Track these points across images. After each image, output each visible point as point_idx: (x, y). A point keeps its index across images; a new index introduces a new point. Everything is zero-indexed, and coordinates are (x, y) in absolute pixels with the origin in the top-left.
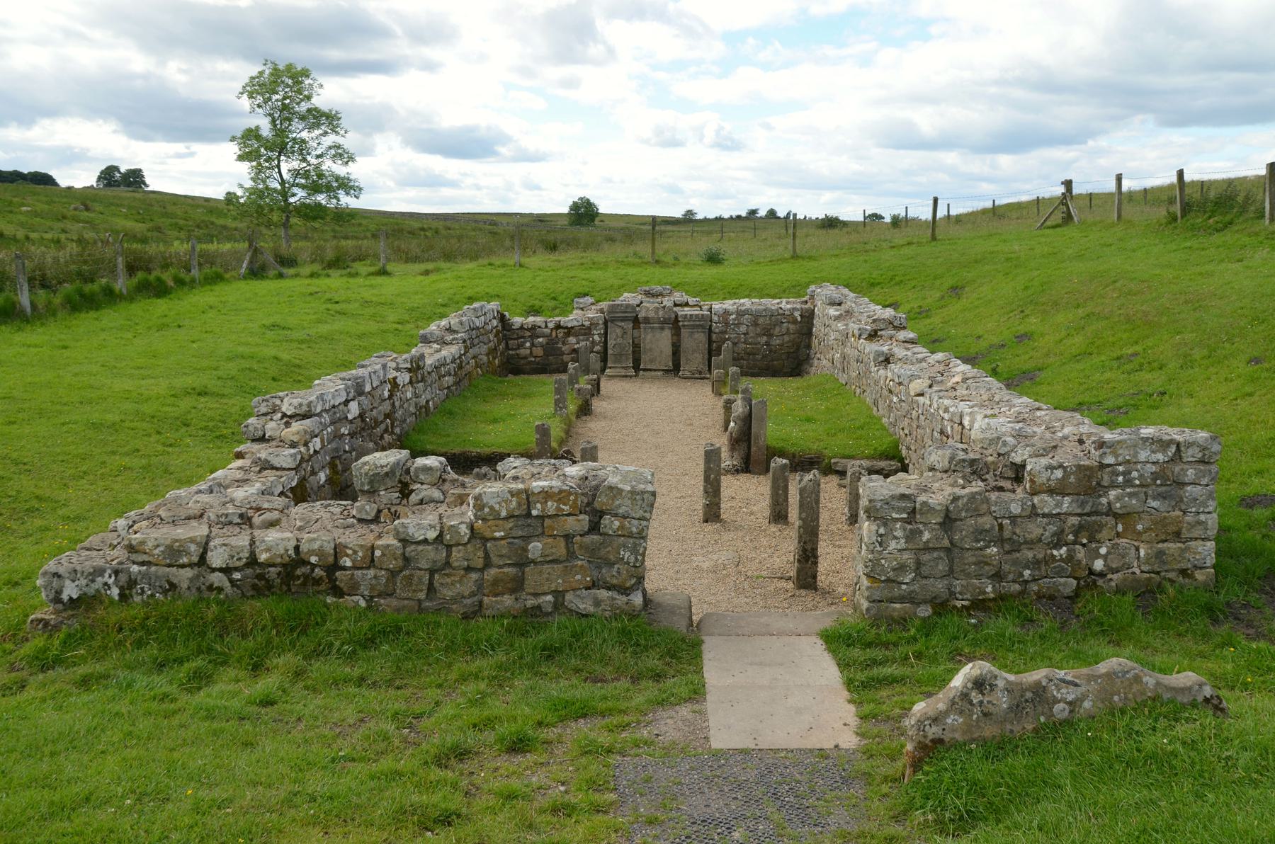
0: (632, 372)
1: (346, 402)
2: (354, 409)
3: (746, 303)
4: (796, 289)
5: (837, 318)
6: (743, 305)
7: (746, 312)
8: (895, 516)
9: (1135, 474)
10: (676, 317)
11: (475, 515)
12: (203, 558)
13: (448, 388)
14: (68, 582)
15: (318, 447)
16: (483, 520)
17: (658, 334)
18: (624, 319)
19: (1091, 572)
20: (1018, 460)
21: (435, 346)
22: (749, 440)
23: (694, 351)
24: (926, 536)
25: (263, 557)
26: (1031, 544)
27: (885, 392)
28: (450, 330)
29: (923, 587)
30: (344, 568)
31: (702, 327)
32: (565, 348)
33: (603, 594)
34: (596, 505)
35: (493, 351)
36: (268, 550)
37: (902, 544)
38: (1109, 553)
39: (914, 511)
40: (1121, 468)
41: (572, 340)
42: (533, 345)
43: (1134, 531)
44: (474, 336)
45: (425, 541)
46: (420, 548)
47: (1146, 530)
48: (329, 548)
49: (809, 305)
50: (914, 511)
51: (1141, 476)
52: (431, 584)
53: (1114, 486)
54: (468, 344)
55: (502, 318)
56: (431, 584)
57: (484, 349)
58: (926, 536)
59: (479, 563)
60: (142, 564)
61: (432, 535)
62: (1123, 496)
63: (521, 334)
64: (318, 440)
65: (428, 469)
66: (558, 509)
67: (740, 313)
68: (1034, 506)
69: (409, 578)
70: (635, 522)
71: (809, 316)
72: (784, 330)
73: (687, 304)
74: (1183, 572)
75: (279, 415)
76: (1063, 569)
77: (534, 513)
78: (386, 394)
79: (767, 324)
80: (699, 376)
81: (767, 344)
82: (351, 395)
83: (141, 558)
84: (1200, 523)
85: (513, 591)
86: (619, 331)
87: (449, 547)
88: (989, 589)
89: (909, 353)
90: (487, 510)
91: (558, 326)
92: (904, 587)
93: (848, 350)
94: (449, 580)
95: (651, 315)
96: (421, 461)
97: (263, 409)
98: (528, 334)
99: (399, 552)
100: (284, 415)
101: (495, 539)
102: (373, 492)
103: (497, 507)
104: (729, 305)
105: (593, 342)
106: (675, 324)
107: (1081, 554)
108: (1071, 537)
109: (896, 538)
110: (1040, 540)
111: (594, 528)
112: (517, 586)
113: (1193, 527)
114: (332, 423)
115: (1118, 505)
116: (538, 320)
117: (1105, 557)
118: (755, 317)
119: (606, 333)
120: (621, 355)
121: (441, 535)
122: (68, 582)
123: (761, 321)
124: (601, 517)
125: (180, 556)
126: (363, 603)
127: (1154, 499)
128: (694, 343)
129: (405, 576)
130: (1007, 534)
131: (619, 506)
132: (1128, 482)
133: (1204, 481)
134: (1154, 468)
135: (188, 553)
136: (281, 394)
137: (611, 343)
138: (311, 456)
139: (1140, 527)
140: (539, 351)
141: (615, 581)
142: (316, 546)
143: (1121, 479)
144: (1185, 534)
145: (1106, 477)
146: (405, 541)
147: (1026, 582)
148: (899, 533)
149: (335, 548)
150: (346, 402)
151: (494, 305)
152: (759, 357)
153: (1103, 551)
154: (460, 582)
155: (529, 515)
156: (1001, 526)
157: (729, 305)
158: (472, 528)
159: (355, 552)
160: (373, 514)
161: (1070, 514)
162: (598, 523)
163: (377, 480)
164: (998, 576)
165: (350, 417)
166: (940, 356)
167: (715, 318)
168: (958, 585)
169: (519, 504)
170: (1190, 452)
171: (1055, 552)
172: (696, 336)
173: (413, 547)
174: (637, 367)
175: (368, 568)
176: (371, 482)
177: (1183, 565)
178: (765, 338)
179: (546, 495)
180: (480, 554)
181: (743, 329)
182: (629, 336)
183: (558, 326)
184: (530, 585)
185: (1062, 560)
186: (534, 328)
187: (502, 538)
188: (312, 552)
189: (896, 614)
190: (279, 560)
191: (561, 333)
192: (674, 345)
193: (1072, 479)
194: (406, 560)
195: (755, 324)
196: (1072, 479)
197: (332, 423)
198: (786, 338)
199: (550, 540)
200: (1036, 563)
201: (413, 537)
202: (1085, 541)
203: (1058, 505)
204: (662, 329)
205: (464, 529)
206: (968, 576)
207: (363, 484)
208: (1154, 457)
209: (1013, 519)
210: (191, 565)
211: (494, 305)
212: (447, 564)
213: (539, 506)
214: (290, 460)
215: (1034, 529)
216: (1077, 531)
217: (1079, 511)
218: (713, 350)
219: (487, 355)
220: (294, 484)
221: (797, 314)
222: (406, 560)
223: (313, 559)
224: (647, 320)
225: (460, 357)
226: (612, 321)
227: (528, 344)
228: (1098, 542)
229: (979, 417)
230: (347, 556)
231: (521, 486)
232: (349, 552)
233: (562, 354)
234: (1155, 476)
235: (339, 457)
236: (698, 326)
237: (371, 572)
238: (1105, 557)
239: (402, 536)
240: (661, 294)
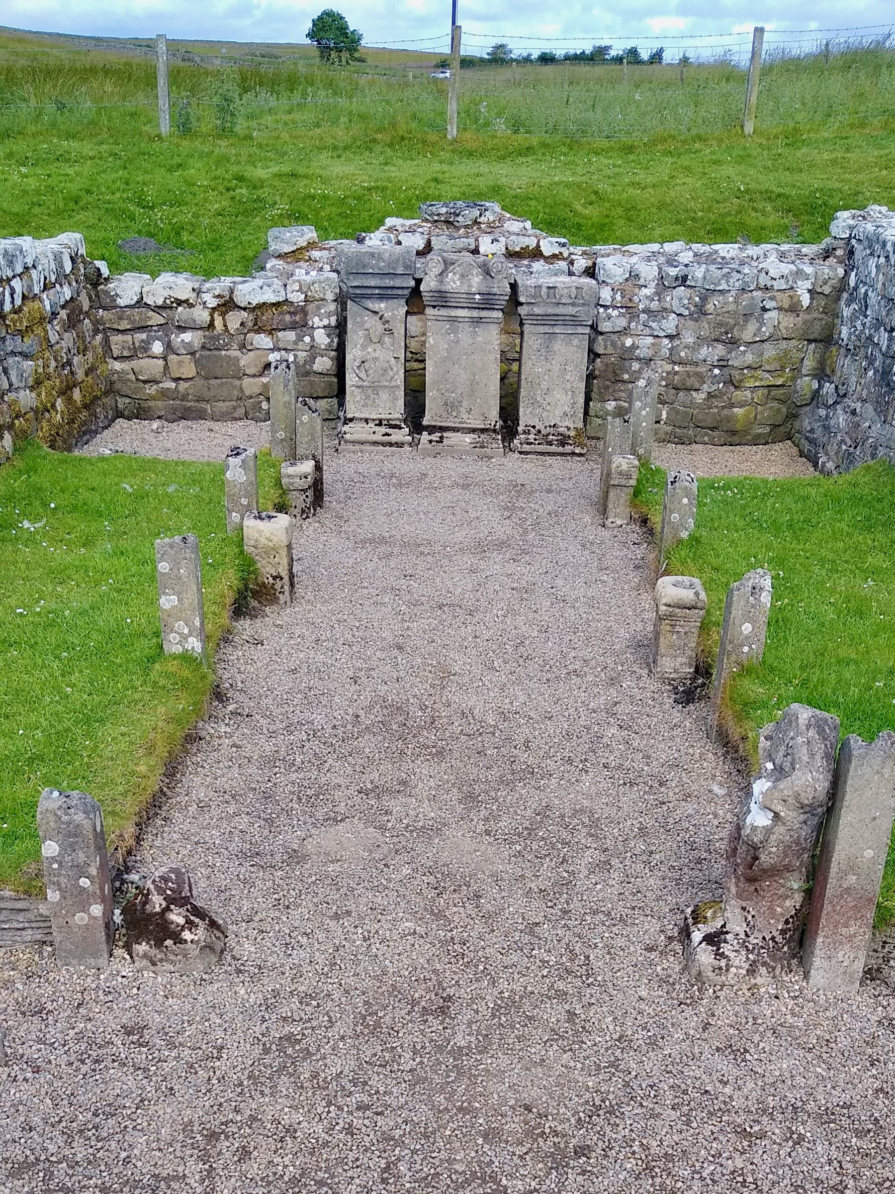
17: (465, 333)
31: (575, 321)
42: (169, 347)
80: (560, 443)
81: (723, 364)
86: (371, 322)
91: (227, 305)
98: (156, 319)
137: (352, 355)
178: (720, 350)
183: (227, 305)
192: (505, 358)
195: (700, 312)
204: (479, 321)
218: (604, 376)
226: (355, 298)
227: (157, 348)
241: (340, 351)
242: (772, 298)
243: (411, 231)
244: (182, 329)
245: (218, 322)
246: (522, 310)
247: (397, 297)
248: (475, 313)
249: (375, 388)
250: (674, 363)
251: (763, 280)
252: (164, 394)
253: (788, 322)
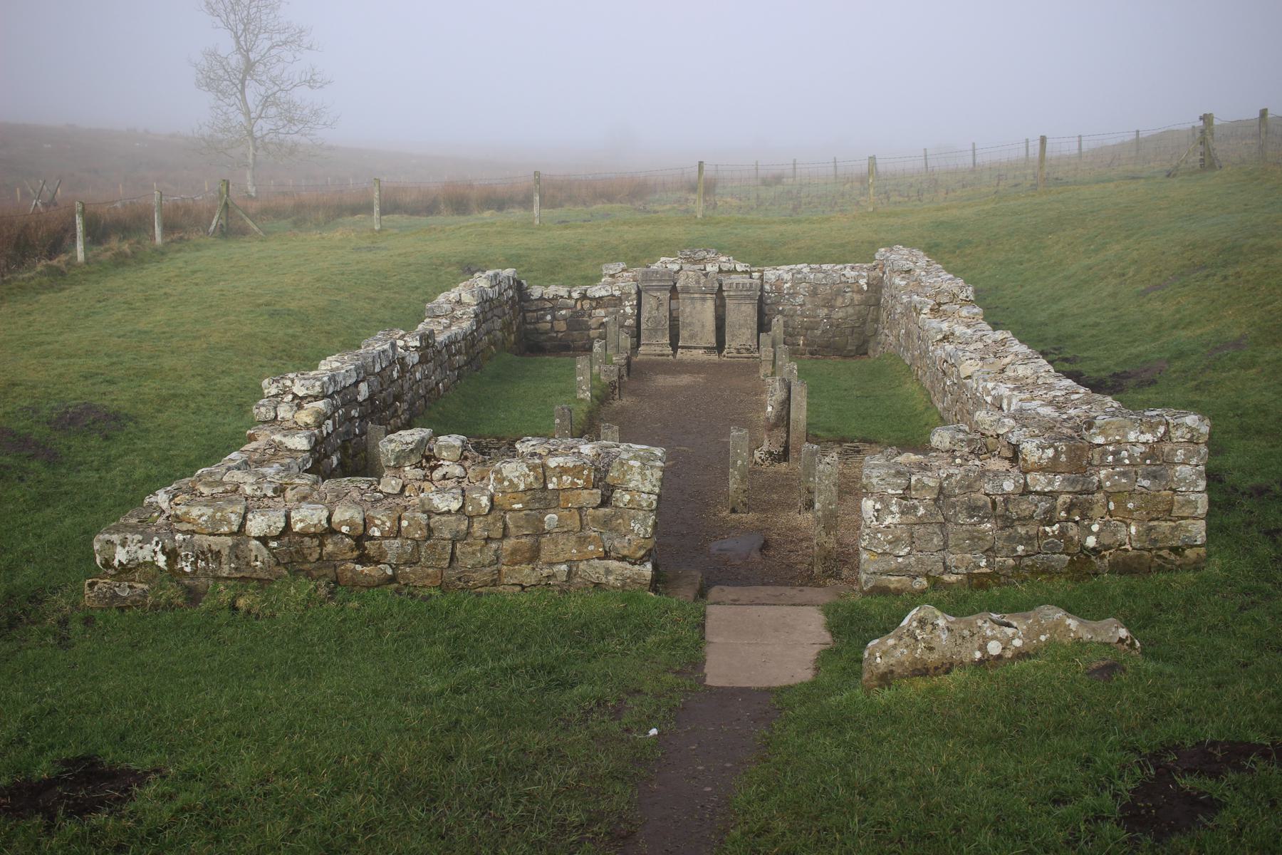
1: (356, 384)
2: (364, 388)
4: (862, 252)
6: (799, 272)
7: (804, 280)
8: (890, 491)
9: (1124, 454)
10: (721, 285)
11: (495, 489)
12: (242, 526)
13: (460, 367)
14: (119, 548)
15: (330, 429)
16: (503, 492)
17: (698, 305)
18: (660, 289)
19: (1083, 548)
20: (1014, 441)
21: (444, 320)
22: (788, 424)
23: (741, 326)
24: (921, 511)
25: (298, 527)
26: (1024, 520)
27: (941, 374)
28: (459, 302)
29: (918, 560)
30: (372, 538)
32: (593, 322)
33: (614, 564)
34: (608, 480)
35: (506, 327)
36: (301, 521)
37: (897, 519)
38: (1101, 530)
39: (908, 488)
40: (1111, 448)
41: (600, 312)
42: (554, 318)
43: (1126, 509)
44: (487, 307)
45: (449, 512)
46: (444, 518)
47: (1138, 508)
48: (359, 519)
49: (878, 273)
50: (908, 488)
51: (1130, 457)
52: (453, 553)
53: (1104, 465)
54: (480, 318)
55: (519, 284)
56: (453, 553)
57: (498, 323)
58: (921, 511)
59: (497, 533)
60: (184, 533)
61: (455, 506)
62: (1113, 475)
63: (540, 305)
64: (330, 422)
65: (448, 447)
66: (573, 483)
68: (1026, 484)
69: (434, 547)
70: (645, 496)
71: (876, 286)
73: (735, 271)
74: (1174, 550)
75: (290, 397)
76: (1056, 545)
77: (550, 486)
78: (395, 375)
81: (828, 317)
82: (362, 375)
83: (185, 527)
84: (1189, 502)
85: (530, 561)
87: (470, 518)
88: (983, 563)
89: (969, 331)
90: (506, 483)
91: (584, 296)
92: (900, 560)
93: (913, 327)
94: (470, 549)
95: (692, 283)
96: (442, 439)
97: (274, 391)
99: (424, 522)
100: (295, 396)
101: (514, 510)
102: (398, 467)
103: (516, 480)
105: (625, 316)
107: (1073, 531)
108: (1063, 514)
109: (892, 513)
110: (1032, 517)
111: (605, 502)
112: (533, 555)
113: (1183, 505)
114: (343, 405)
115: (1108, 484)
116: (563, 291)
117: (1097, 535)
119: (639, 305)
121: (463, 507)
122: (119, 548)
124: (613, 491)
125: (222, 526)
126: (389, 572)
127: (1144, 478)
129: (430, 546)
130: (1000, 510)
131: (630, 480)
132: (1118, 462)
133: (1194, 461)
134: (1143, 449)
135: (230, 523)
136: (291, 375)
137: (645, 315)
138: (324, 439)
139: (1130, 505)
140: (562, 326)
141: (625, 552)
142: (347, 516)
143: (1110, 458)
144: (1176, 512)
145: (1096, 456)
146: (430, 513)
147: (1021, 557)
148: (894, 508)
149: (364, 520)
150: (356, 384)
151: (509, 272)
152: (818, 332)
153: (1095, 528)
154: (481, 551)
155: (545, 487)
156: (994, 503)
157: (784, 272)
158: (492, 500)
159: (384, 523)
160: (398, 489)
161: (1061, 493)
162: (609, 498)
163: (401, 458)
164: (990, 552)
165: (360, 399)
166: (999, 335)
167: (767, 287)
168: (952, 559)
169: (536, 478)
170: (1179, 433)
171: (1048, 529)
172: (743, 308)
173: (437, 518)
175: (395, 538)
176: (397, 458)
177: (1174, 543)
178: (826, 311)
179: (563, 470)
180: (500, 524)
181: (800, 299)
182: (666, 307)
183: (584, 296)
184: (545, 555)
185: (1054, 536)
186: (556, 298)
187: (520, 510)
188: (342, 523)
189: (892, 586)
190: (313, 530)
191: (586, 304)
193: (1063, 458)
194: (430, 530)
195: (814, 293)
196: (1063, 458)
197: (343, 405)
198: (850, 310)
199: (566, 512)
200: (1028, 540)
201: (437, 508)
202: (1077, 518)
203: (1050, 483)
204: (704, 299)
205: (485, 501)
206: (963, 551)
207: (389, 460)
208: (1143, 438)
209: (1007, 498)
210: (231, 534)
211: (509, 272)
212: (468, 533)
213: (554, 479)
214: (305, 442)
215: (1025, 507)
216: (1069, 508)
217: (1070, 489)
219: (501, 330)
220: (308, 466)
221: (863, 282)
222: (430, 530)
223: (345, 529)
224: (686, 290)
225: (472, 333)
227: (549, 317)
228: (1091, 519)
229: (1014, 401)
230: (376, 526)
231: (537, 461)
232: (378, 522)
233: (589, 328)
234: (1144, 456)
235: (350, 441)
236: (746, 297)
237: (397, 543)
238: (1097, 535)
239: (427, 508)
241: (639, 315)
243: (673, 262)
244: (562, 309)
245: (579, 306)
246: (725, 294)
249: (656, 330)
251: (843, 279)
252: (552, 339)
253: (857, 297)
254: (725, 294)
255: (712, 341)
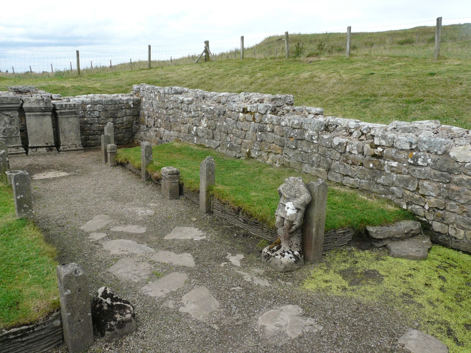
0: (22, 150)
3: (97, 97)
5: (190, 103)
18: (9, 109)
23: (70, 131)
49: (135, 97)
67: (94, 103)
72: (123, 114)
79: (111, 110)
104: (83, 98)
106: (54, 113)
118: (105, 105)
120: (11, 137)
123: (109, 108)
128: (69, 127)
172: (71, 120)
174: (25, 145)
181: (96, 113)
221: (131, 103)
224: (31, 110)
240: (28, 91)
242: (124, 106)
247: (15, 110)
248: (42, 113)
250: (100, 124)
254: (58, 112)
255: (52, 142)
